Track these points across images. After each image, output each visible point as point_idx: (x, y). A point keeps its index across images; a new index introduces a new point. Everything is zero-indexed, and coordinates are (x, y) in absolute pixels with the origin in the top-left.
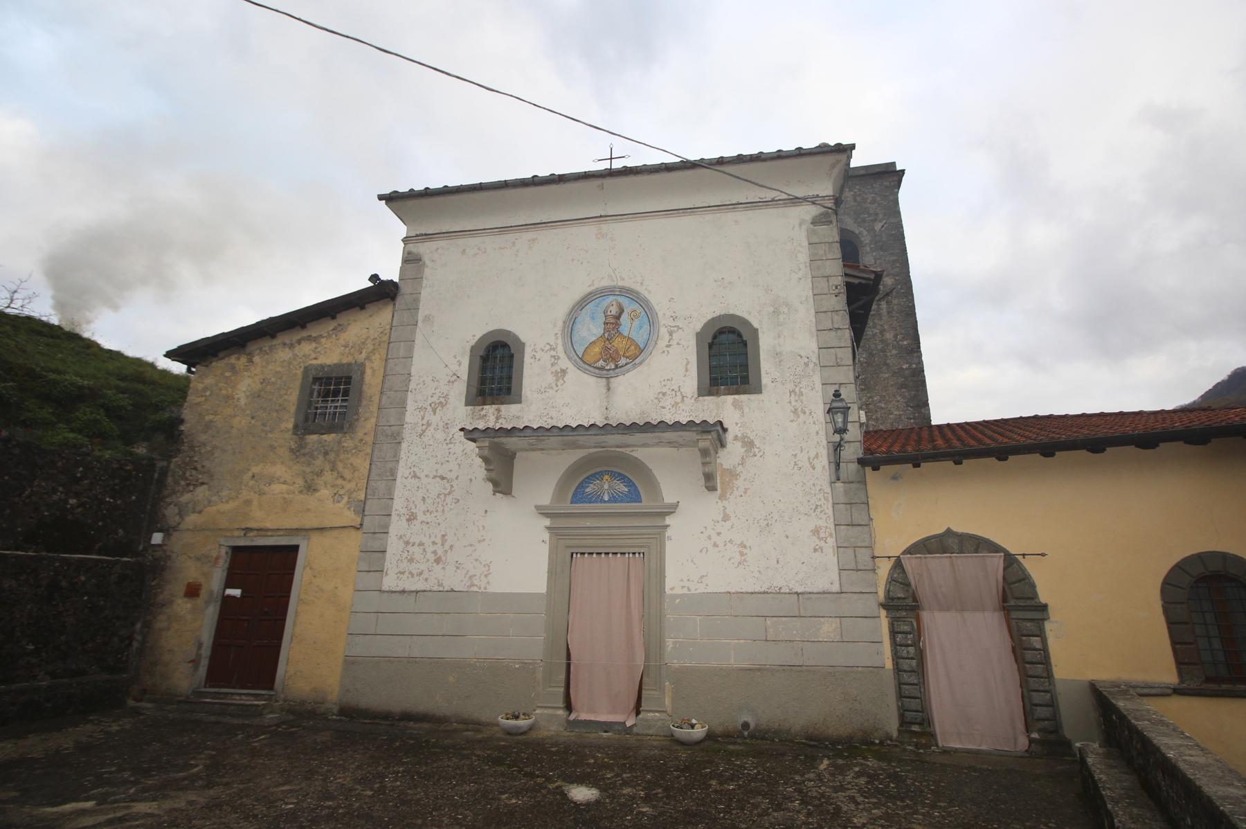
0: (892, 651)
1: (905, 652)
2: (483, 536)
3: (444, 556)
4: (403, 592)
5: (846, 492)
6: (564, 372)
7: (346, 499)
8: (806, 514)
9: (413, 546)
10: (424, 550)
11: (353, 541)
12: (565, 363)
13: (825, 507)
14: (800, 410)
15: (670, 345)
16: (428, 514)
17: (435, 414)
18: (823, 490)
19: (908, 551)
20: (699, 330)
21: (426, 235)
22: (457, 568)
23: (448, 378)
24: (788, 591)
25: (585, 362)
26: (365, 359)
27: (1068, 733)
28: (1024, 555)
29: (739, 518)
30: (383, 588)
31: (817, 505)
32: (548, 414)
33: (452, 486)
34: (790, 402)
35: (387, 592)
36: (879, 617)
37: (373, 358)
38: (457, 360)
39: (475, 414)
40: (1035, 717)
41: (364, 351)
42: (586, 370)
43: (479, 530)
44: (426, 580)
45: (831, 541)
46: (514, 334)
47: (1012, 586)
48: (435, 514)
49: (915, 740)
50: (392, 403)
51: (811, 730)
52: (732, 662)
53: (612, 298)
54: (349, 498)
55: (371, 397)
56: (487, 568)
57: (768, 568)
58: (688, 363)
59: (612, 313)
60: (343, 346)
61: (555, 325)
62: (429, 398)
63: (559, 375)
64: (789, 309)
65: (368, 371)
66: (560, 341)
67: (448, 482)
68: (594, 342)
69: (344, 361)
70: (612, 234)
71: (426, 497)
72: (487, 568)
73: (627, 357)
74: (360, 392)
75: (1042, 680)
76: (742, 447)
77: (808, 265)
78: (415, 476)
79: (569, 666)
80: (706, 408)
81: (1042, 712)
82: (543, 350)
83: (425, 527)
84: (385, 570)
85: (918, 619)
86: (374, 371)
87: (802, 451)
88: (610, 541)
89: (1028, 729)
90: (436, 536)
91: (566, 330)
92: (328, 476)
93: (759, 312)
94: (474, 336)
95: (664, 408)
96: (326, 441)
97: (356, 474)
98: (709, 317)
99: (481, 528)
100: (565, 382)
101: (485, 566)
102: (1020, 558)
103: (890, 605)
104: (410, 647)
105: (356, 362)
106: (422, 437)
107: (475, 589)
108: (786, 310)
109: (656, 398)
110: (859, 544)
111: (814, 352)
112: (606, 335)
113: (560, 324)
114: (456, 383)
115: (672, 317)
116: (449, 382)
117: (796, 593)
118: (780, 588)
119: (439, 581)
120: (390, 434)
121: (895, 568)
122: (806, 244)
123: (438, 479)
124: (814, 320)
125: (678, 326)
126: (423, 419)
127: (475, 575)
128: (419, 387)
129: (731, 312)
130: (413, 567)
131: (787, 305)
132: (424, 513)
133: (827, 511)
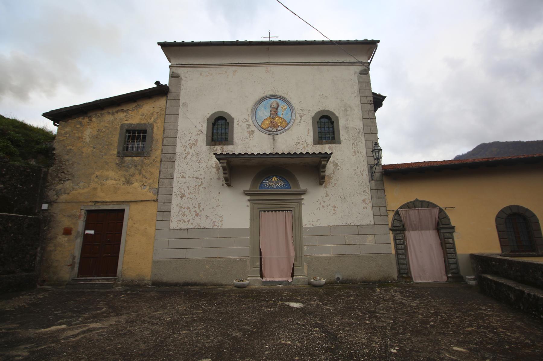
0: (395, 247)
1: (400, 247)
2: (218, 204)
3: (200, 213)
4: (181, 229)
5: (376, 185)
6: (253, 132)
7: (148, 187)
8: (360, 194)
9: (184, 208)
10: (190, 210)
11: (152, 208)
12: (253, 128)
13: (367, 191)
14: (356, 151)
15: (301, 122)
16: (191, 194)
17: (191, 149)
18: (367, 184)
19: (401, 208)
20: (313, 116)
21: (181, 64)
22: (207, 218)
23: (197, 132)
24: (353, 225)
25: (262, 128)
26: (153, 122)
27: (462, 274)
28: (445, 208)
29: (333, 196)
30: (171, 228)
31: (364, 190)
32: (246, 150)
33: (202, 182)
34: (352, 148)
35: (173, 229)
36: (389, 234)
37: (157, 121)
38: (200, 124)
39: (211, 149)
40: (450, 268)
41: (152, 118)
42: (263, 131)
43: (216, 201)
44: (192, 224)
45: (370, 204)
46: (228, 113)
47: (442, 220)
48: (194, 194)
49: (405, 280)
50: (169, 143)
51: (364, 279)
52: (332, 254)
53: (273, 100)
54: (150, 187)
55: (157, 140)
56: (221, 218)
57: (345, 215)
58: (309, 130)
59: (274, 106)
60: (141, 115)
61: (248, 111)
62: (188, 141)
63: (251, 133)
64: (351, 109)
65: (155, 129)
66: (250, 118)
67: (200, 180)
68: (266, 119)
69: (143, 122)
70: (273, 71)
71: (189, 186)
72: (221, 218)
73: (281, 126)
74: (152, 137)
75: (453, 254)
76: (333, 166)
77: (358, 91)
78: (183, 177)
79: (261, 259)
80: (317, 149)
81: (453, 266)
82: (242, 122)
83: (190, 200)
84: (171, 220)
85: (404, 234)
86: (158, 128)
87: (358, 168)
89: (447, 272)
90: (195, 204)
91: (253, 113)
92: (138, 177)
93: (339, 110)
94: (209, 113)
95: (299, 149)
96: (135, 160)
97: (152, 176)
98: (317, 111)
99: (217, 200)
100: (253, 136)
101: (220, 217)
102: (444, 209)
103: (394, 229)
104: (186, 254)
105: (148, 123)
106: (185, 159)
107: (216, 227)
108: (350, 109)
109: (295, 145)
110: (381, 206)
111: (362, 128)
112: (272, 116)
113: (250, 110)
114: (200, 135)
115: (301, 109)
116: (197, 134)
117: (357, 225)
118: (350, 224)
119: (198, 224)
120: (169, 157)
121: (396, 215)
122: (357, 82)
123: (195, 178)
124: (361, 114)
125: (304, 114)
126: (185, 151)
127: (216, 221)
128: (182, 136)
129: (327, 109)
130: (185, 218)
131: (350, 107)
132: (189, 194)
133: (368, 193)
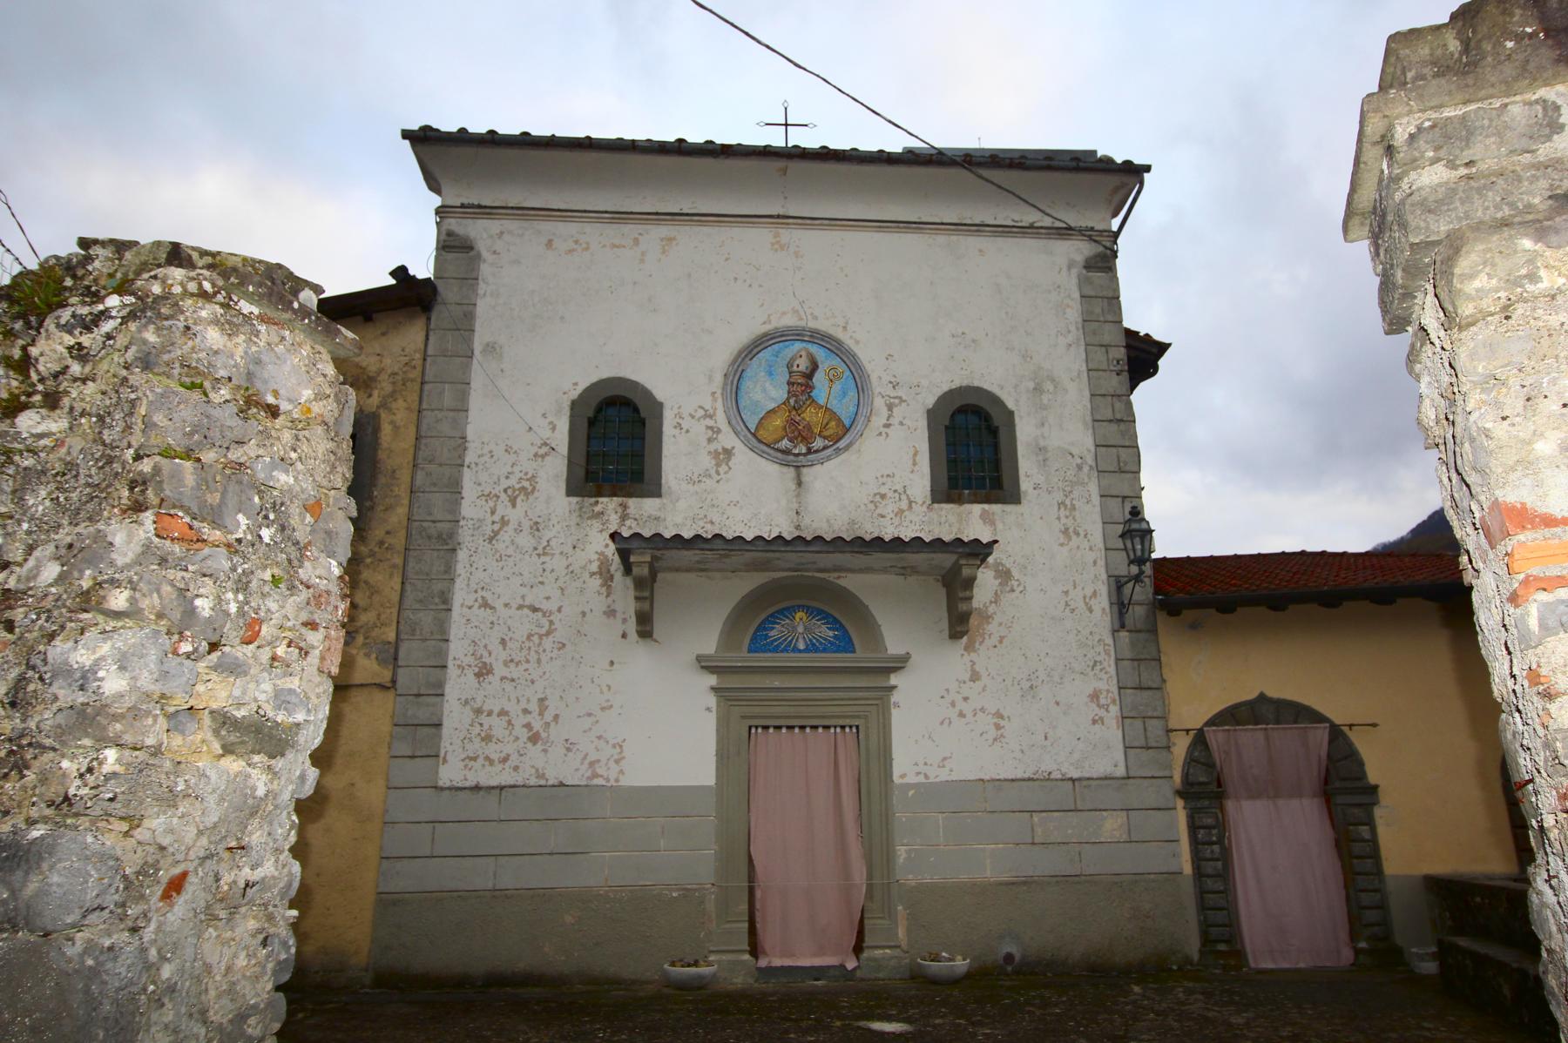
2: (608, 701)
6: (728, 453)
10: (509, 723)
12: (728, 439)
16: (512, 665)
17: (514, 506)
19: (1211, 722)
21: (480, 206)
22: (568, 750)
23: (534, 450)
24: (1060, 776)
25: (759, 440)
26: (378, 407)
27: (1399, 939)
28: (1351, 726)
29: (993, 678)
30: (441, 783)
31: (1096, 662)
32: (705, 516)
33: (551, 622)
35: (450, 789)
37: (394, 405)
38: (548, 420)
41: (376, 393)
43: (602, 692)
45: (1114, 709)
46: (643, 387)
48: (526, 666)
49: (1222, 962)
50: (435, 485)
53: (798, 346)
54: (366, 638)
55: (394, 471)
56: (618, 750)
58: (916, 454)
59: (801, 368)
61: (710, 378)
63: (721, 456)
64: (1056, 387)
65: (386, 430)
66: (719, 404)
67: (544, 615)
70: (798, 247)
71: (507, 639)
73: (825, 438)
76: (995, 578)
77: (1080, 326)
78: (485, 605)
80: (943, 519)
81: (1371, 916)
82: (693, 417)
83: (508, 686)
84: (442, 755)
85: (1222, 808)
86: (396, 428)
87: (1075, 588)
88: (834, 709)
89: (1353, 936)
90: (528, 701)
91: (729, 388)
94: (576, 384)
95: (883, 516)
97: (376, 598)
98: (946, 388)
99: (605, 689)
100: (730, 468)
101: (614, 746)
102: (1346, 729)
103: (1189, 792)
104: (495, 875)
106: (494, 542)
108: (1051, 388)
109: (872, 502)
110: (1150, 714)
111: (1089, 451)
112: (792, 401)
113: (719, 379)
114: (547, 458)
115: (891, 382)
116: (536, 455)
118: (1050, 773)
119: (537, 770)
122: (1077, 295)
123: (526, 611)
124: (1089, 407)
125: (900, 398)
126: (493, 513)
127: (599, 761)
128: (482, 460)
129: (976, 383)
130: (493, 750)
131: (1053, 380)
132: (506, 664)
133: (1108, 669)
